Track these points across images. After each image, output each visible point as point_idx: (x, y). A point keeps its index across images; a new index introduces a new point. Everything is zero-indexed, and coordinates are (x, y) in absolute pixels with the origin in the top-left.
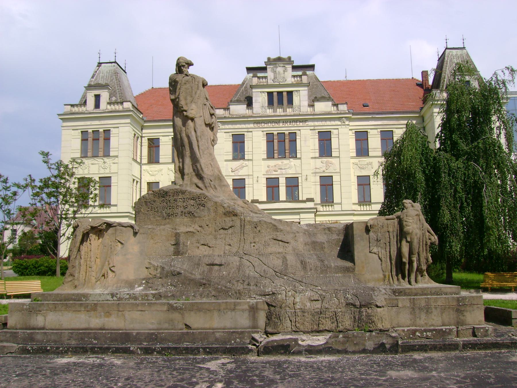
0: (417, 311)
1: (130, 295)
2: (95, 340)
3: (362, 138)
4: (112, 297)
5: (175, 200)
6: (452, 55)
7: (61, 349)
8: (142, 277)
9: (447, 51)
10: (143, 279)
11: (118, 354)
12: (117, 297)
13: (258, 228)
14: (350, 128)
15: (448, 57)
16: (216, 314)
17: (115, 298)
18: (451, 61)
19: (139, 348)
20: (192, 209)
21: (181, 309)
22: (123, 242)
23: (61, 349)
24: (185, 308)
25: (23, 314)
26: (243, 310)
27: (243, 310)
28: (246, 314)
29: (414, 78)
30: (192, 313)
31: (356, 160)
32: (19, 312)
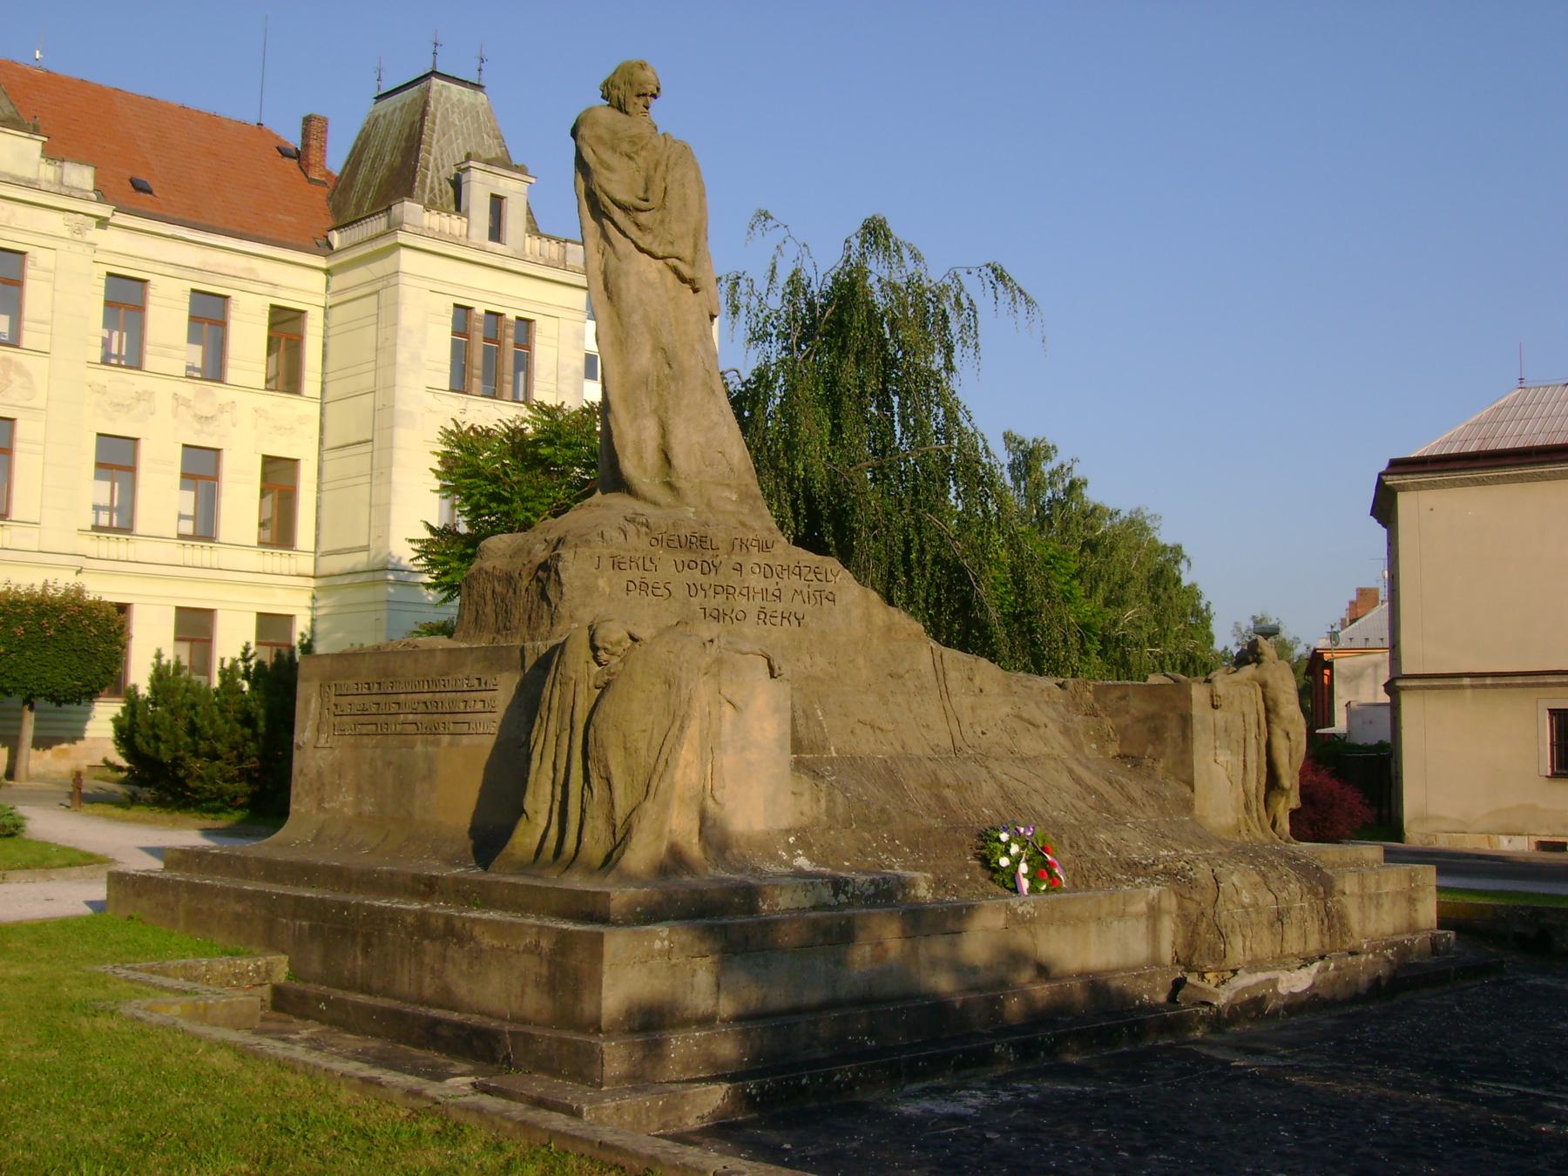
0: (1366, 901)
1: (877, 886)
2: (870, 1039)
3: (125, 299)
4: (836, 895)
5: (739, 568)
6: (448, 98)
7: (837, 1077)
8: (784, 823)
9: (436, 82)
10: (788, 832)
11: (968, 1072)
12: (846, 893)
13: (977, 681)
14: (98, 257)
15: (437, 101)
16: (1093, 928)
17: (842, 898)
18: (445, 117)
19: (1011, 1044)
20: (797, 606)
21: (1032, 921)
22: (738, 703)
23: (837, 1077)
24: (1040, 916)
25: (651, 971)
26: (1137, 916)
27: (1137, 916)
28: (1142, 926)
29: (267, 124)
30: (1052, 929)
31: (189, 389)
32: (637, 967)
